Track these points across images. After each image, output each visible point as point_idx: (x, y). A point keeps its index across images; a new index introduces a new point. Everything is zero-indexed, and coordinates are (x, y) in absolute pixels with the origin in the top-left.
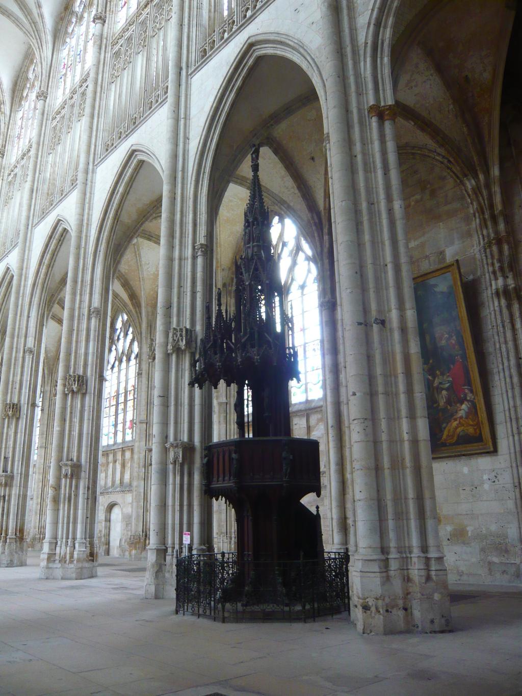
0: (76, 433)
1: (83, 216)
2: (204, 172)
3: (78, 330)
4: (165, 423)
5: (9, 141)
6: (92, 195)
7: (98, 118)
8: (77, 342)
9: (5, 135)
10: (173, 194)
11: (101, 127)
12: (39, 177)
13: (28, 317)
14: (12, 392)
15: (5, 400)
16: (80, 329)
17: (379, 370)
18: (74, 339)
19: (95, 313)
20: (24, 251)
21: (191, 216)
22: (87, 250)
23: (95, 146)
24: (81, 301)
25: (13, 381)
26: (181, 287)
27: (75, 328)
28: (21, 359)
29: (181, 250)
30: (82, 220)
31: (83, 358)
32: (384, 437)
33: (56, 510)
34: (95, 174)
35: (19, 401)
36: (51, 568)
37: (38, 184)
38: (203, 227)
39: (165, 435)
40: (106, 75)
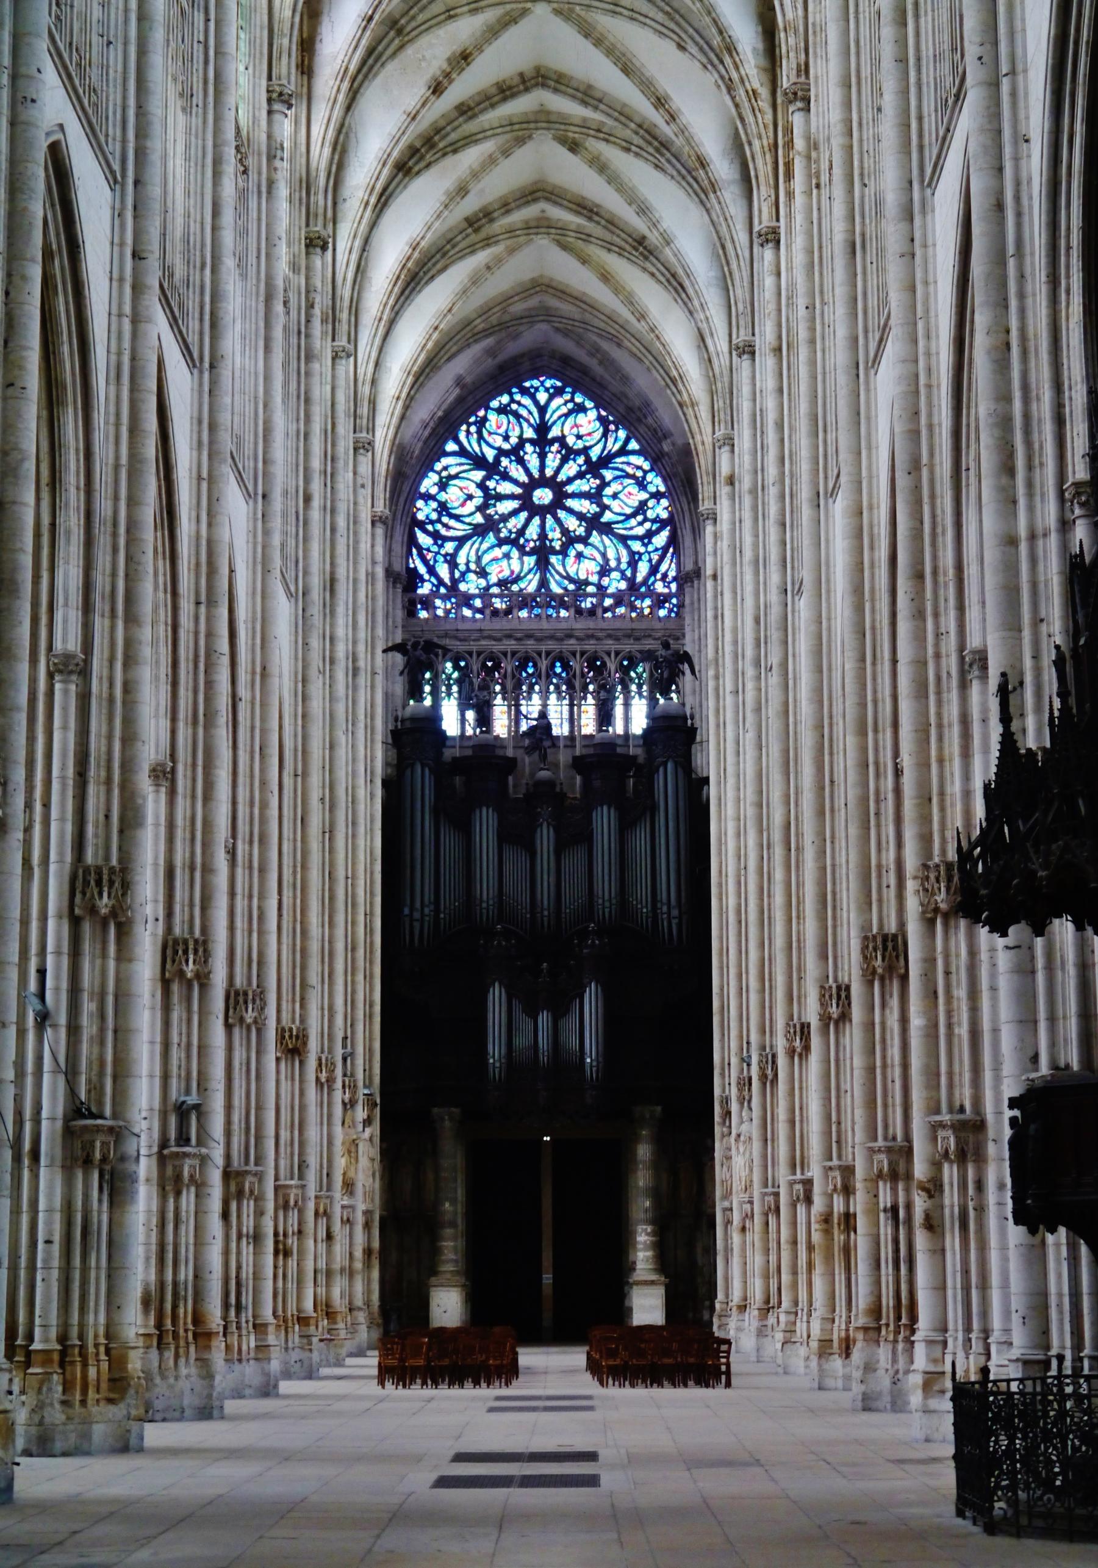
0: (963, 1031)
1: (916, 361)
2: (1069, 248)
3: (940, 726)
4: (1027, 1022)
5: (815, 44)
6: (931, 288)
7: (917, 16)
8: (941, 761)
9: (801, 29)
10: (1003, 336)
11: (927, 51)
12: (862, 197)
14: (880, 901)
15: (866, 927)
16: (945, 721)
18: (933, 753)
19: (975, 667)
20: (859, 453)
22: (937, 469)
23: (920, 119)
24: (938, 635)
25: (879, 866)
26: (1042, 620)
27: (933, 719)
28: (890, 796)
29: (1031, 509)
30: (917, 376)
31: (959, 807)
34: (929, 217)
35: (902, 925)
36: (934, 1411)
37: (863, 223)
38: (1081, 426)
39: (1032, 1054)
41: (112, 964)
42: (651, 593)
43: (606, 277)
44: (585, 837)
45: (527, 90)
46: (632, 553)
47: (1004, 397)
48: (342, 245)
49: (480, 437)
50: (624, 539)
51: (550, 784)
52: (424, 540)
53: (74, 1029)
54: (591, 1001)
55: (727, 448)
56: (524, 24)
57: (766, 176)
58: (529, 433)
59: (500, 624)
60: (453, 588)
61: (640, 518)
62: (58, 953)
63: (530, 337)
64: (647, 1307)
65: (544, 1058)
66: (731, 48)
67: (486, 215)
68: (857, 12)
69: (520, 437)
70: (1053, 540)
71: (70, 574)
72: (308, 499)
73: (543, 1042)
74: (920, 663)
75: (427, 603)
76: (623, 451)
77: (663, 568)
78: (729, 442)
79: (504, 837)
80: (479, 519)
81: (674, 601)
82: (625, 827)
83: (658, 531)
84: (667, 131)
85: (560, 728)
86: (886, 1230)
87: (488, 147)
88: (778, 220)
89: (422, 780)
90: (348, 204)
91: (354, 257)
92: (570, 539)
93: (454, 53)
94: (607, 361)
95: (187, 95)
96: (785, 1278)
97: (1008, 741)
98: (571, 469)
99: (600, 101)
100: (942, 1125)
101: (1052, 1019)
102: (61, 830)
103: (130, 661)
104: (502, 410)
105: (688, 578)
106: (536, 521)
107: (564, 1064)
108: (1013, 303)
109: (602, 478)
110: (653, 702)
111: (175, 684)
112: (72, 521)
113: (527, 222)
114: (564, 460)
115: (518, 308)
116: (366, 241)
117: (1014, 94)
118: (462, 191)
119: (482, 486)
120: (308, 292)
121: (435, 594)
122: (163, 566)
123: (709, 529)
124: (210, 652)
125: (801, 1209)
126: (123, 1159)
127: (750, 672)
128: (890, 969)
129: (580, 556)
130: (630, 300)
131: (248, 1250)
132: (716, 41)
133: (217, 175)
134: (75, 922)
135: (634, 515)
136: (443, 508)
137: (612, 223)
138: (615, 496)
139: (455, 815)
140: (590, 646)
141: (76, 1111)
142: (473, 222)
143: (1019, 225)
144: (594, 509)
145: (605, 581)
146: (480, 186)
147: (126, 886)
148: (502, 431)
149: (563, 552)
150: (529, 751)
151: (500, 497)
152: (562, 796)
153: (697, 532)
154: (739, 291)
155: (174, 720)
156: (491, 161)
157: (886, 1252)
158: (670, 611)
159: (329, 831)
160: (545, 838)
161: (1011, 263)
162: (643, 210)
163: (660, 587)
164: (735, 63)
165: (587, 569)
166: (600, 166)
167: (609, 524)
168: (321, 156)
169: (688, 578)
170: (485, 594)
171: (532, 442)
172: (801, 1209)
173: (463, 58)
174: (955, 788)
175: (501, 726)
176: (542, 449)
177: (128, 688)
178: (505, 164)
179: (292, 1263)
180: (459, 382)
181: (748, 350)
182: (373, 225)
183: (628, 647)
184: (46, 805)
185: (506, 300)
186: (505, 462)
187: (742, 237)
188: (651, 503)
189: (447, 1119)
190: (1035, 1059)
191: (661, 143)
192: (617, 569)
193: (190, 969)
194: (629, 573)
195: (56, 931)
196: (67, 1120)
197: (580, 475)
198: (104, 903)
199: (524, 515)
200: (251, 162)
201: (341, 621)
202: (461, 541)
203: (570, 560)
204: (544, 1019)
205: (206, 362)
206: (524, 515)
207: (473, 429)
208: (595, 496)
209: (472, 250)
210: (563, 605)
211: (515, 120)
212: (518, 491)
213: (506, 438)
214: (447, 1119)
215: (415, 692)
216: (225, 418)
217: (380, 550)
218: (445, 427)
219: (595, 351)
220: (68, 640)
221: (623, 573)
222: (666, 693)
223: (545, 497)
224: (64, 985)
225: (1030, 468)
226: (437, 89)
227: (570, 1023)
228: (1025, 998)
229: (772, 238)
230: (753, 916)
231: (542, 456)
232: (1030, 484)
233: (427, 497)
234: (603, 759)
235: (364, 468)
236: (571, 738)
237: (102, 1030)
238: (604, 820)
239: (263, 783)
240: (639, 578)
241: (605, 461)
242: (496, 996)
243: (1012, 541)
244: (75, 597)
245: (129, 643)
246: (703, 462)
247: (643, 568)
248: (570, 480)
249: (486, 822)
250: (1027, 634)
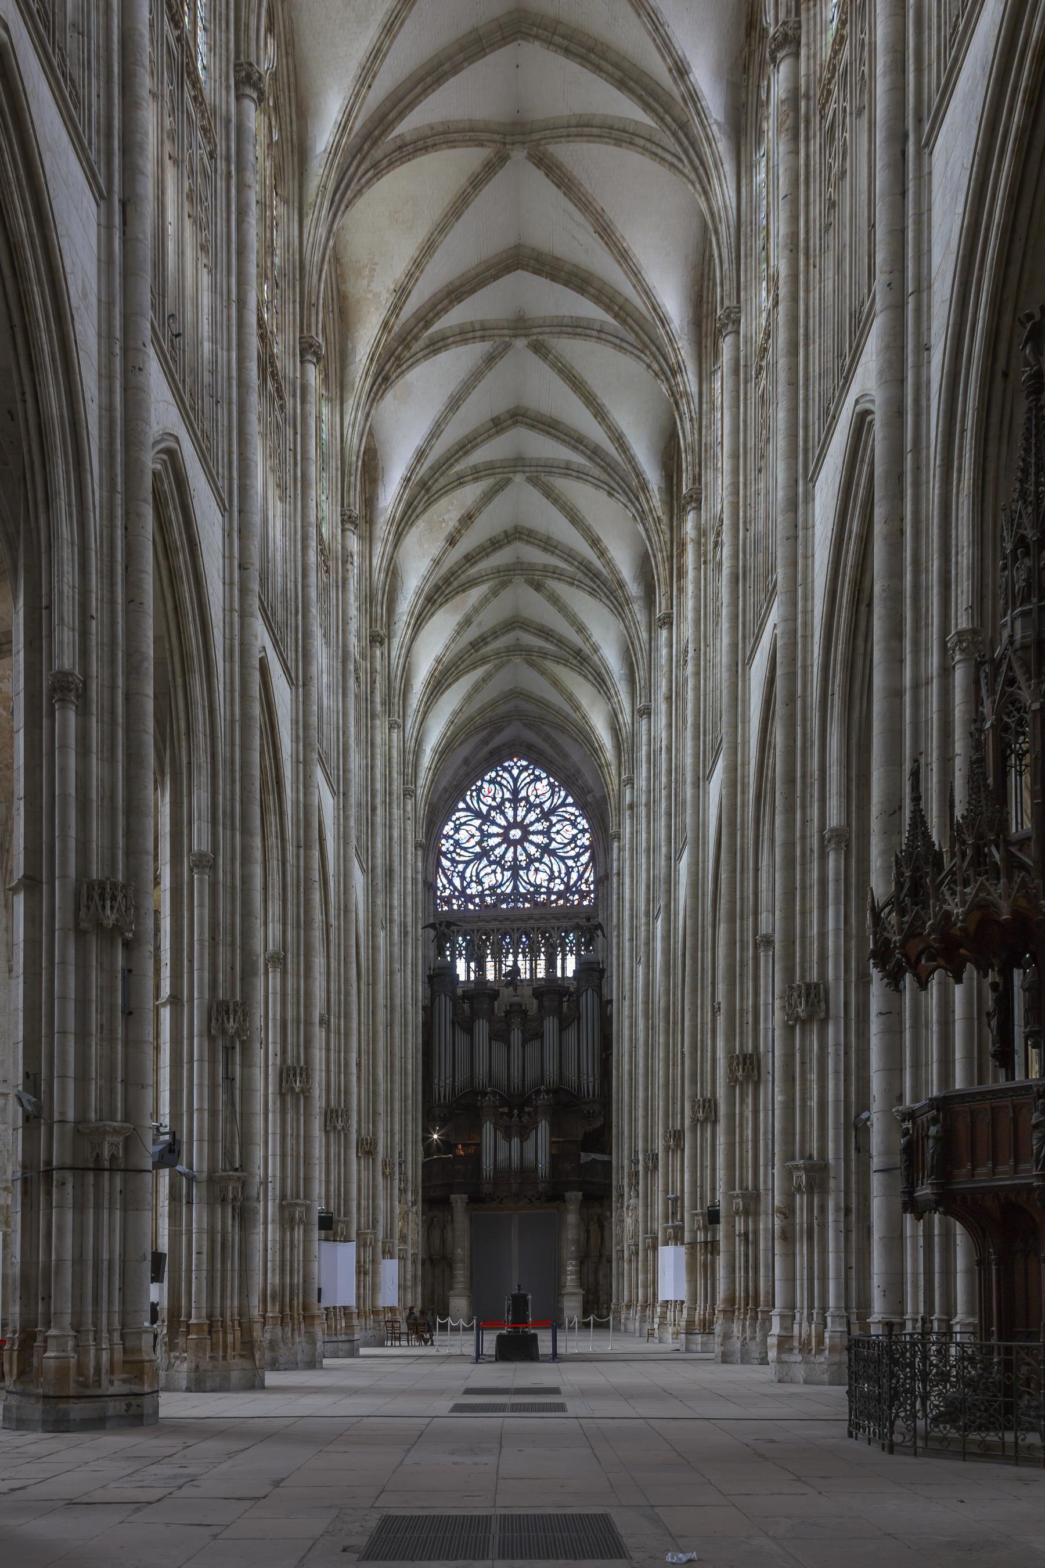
45: (509, 542)
46: (567, 867)
49: (479, 799)
50: (563, 859)
55: (629, 786)
57: (665, 578)
58: (507, 795)
61: (573, 845)
68: (745, 399)
69: (502, 798)
77: (586, 876)
78: (631, 781)
81: (592, 896)
83: (583, 853)
88: (672, 608)
90: (397, 626)
91: (401, 660)
93: (462, 516)
98: (532, 816)
99: (556, 548)
106: (512, 849)
109: (551, 821)
113: (508, 647)
114: (528, 812)
116: (409, 650)
119: (479, 829)
120: (371, 673)
123: (616, 844)
129: (537, 870)
135: (569, 844)
138: (558, 832)
144: (546, 841)
145: (552, 885)
146: (479, 619)
148: (491, 794)
149: (527, 868)
153: (608, 850)
154: (642, 673)
158: (590, 901)
160: (516, 1036)
163: (584, 887)
164: (646, 498)
165: (542, 878)
167: (554, 850)
169: (602, 880)
171: (509, 800)
176: (515, 805)
181: (646, 712)
182: (413, 639)
186: (493, 814)
188: (579, 836)
191: (594, 575)
192: (559, 877)
194: (565, 880)
197: (538, 820)
199: (504, 846)
203: (531, 873)
206: (504, 846)
207: (474, 794)
211: (501, 569)
212: (501, 831)
213: (494, 799)
221: (562, 879)
229: (667, 621)
231: (515, 810)
240: (572, 883)
241: (553, 811)
247: (574, 876)
248: (532, 824)
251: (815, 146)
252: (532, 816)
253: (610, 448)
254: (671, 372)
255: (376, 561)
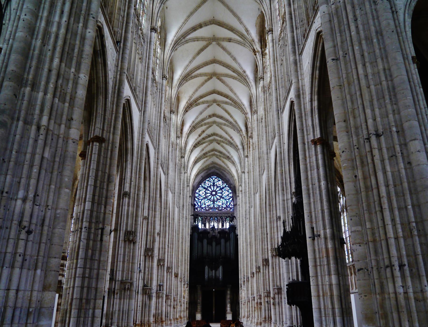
0: (278, 274)
4: (288, 273)
8: (274, 233)
11: (270, 131)
13: (266, 218)
15: (263, 258)
17: (317, 256)
21: (289, 179)
24: (273, 214)
32: (320, 283)
33: (275, 309)
35: (268, 257)
40: (268, 105)
41: (150, 263)
42: (229, 207)
43: (223, 162)
44: (220, 244)
47: (282, 180)
48: (186, 157)
50: (226, 199)
51: (215, 235)
52: (196, 199)
53: (144, 273)
54: (221, 268)
56: (212, 127)
58: (212, 184)
59: (207, 212)
60: (201, 206)
62: (143, 261)
63: (212, 170)
64: (229, 317)
65: (214, 278)
66: (241, 130)
67: (206, 153)
70: (290, 200)
71: (146, 205)
72: (180, 194)
73: (213, 275)
74: (270, 218)
75: (197, 209)
76: (225, 187)
78: (241, 185)
79: (208, 243)
80: (204, 196)
82: (226, 242)
84: (232, 142)
85: (216, 227)
86: (266, 305)
87: (207, 144)
89: (196, 235)
92: (218, 199)
94: (223, 174)
95: (165, 137)
96: (251, 312)
97: (285, 230)
98: (218, 189)
100: (275, 288)
101: (292, 272)
102: (144, 243)
103: (155, 217)
104: (208, 181)
105: (235, 205)
107: (217, 278)
108: (283, 166)
110: (230, 223)
111: (161, 221)
112: (147, 197)
114: (217, 188)
115: (211, 166)
117: (283, 137)
118: (203, 150)
119: (205, 192)
121: (198, 207)
122: (160, 203)
124: (166, 216)
125: (253, 301)
126: (151, 293)
127: (244, 219)
128: (266, 264)
129: (219, 202)
130: (227, 165)
131: (169, 308)
132: (239, 129)
133: (169, 148)
134: (145, 257)
136: (199, 195)
137: (224, 154)
139: (201, 240)
140: (221, 215)
141: (144, 286)
142: (204, 154)
143: (284, 156)
147: (153, 251)
149: (217, 201)
150: (212, 230)
151: (208, 193)
152: (216, 237)
153: (236, 198)
155: (160, 226)
156: (207, 146)
157: (267, 308)
159: (182, 243)
160: (214, 244)
161: (283, 161)
162: (229, 153)
163: (231, 206)
165: (220, 204)
166: (223, 147)
168: (183, 145)
169: (235, 205)
170: (205, 207)
172: (253, 301)
173: (204, 132)
174: (276, 237)
175: (207, 227)
177: (154, 221)
178: (209, 146)
179: (175, 310)
180: (202, 177)
181: (244, 172)
182: (190, 154)
183: (226, 215)
184: (142, 239)
185: (209, 165)
187: (243, 156)
189: (199, 287)
190: (290, 278)
193: (162, 264)
195: (142, 258)
196: (143, 287)
197: (219, 190)
198: (150, 254)
200: (173, 146)
201: (184, 211)
202: (202, 200)
204: (214, 271)
205: (167, 174)
208: (221, 193)
209: (204, 158)
210: (217, 209)
214: (199, 287)
215: (195, 222)
216: (169, 182)
217: (190, 201)
218: (200, 183)
219: (222, 172)
220: (146, 214)
222: (232, 222)
223: (214, 193)
224: (143, 266)
225: (286, 190)
226: (200, 136)
227: (218, 272)
228: (288, 269)
229: (247, 157)
230: (245, 256)
231: (214, 187)
232: (286, 192)
233: (197, 193)
234: (222, 232)
235: (188, 189)
236: (218, 229)
237: (149, 273)
238: (223, 241)
239: (173, 235)
241: (223, 188)
242: (206, 268)
243: (284, 200)
244: (147, 208)
245: (154, 215)
246: (237, 188)
247: (228, 204)
249: (205, 241)
250: (286, 214)
251: (267, 95)
252: (218, 189)
253: (234, 123)
254: (246, 114)
255: (183, 141)
